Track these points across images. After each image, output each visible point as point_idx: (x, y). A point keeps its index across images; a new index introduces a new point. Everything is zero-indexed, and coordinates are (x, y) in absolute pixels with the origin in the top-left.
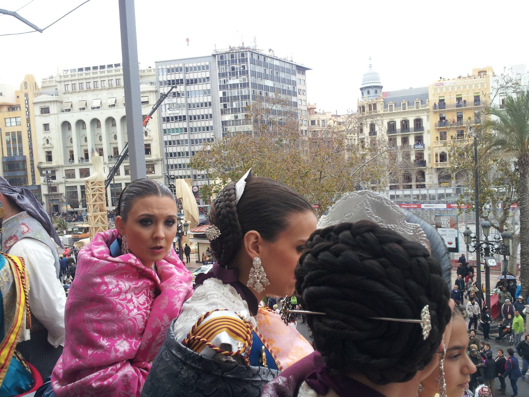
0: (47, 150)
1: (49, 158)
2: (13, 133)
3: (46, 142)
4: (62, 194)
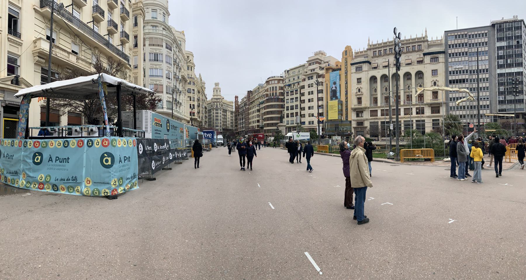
0: (358, 96)
1: (359, 100)
4: (366, 127)
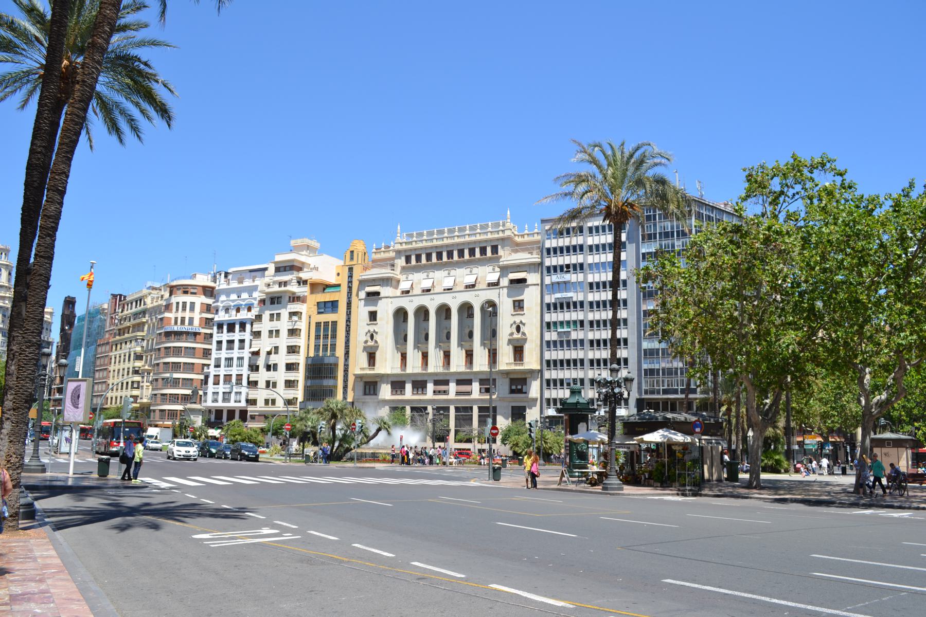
2: (326, 323)
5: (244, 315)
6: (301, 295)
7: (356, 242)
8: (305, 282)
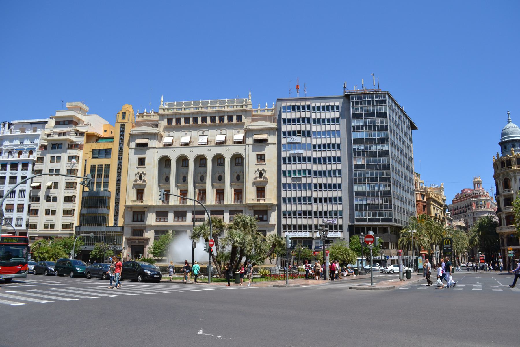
2: (100, 166)
3: (138, 178)
5: (24, 157)
6: (79, 143)
7: (126, 106)
8: (81, 134)
